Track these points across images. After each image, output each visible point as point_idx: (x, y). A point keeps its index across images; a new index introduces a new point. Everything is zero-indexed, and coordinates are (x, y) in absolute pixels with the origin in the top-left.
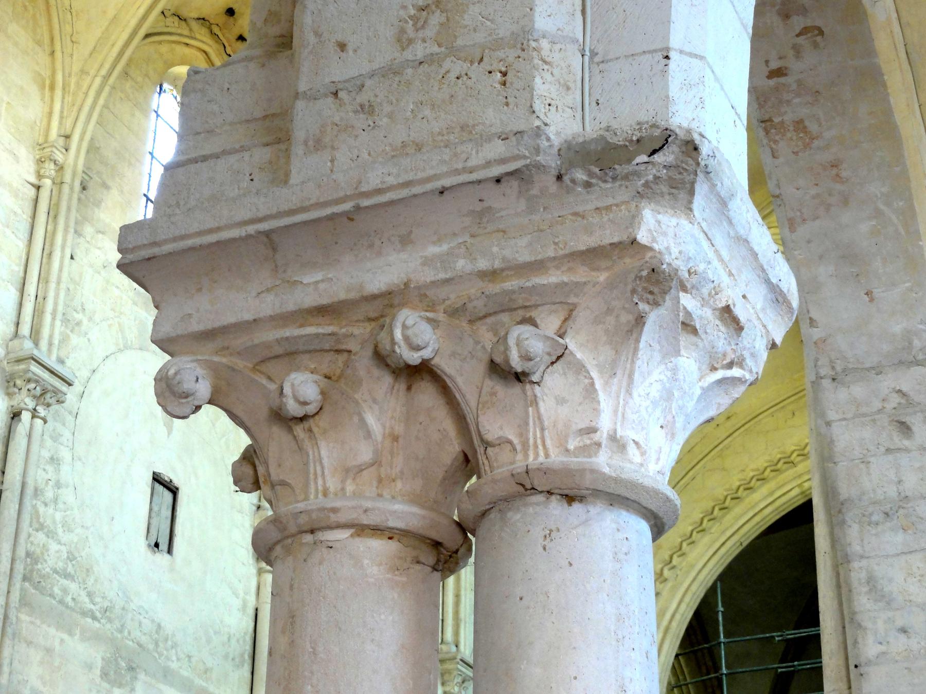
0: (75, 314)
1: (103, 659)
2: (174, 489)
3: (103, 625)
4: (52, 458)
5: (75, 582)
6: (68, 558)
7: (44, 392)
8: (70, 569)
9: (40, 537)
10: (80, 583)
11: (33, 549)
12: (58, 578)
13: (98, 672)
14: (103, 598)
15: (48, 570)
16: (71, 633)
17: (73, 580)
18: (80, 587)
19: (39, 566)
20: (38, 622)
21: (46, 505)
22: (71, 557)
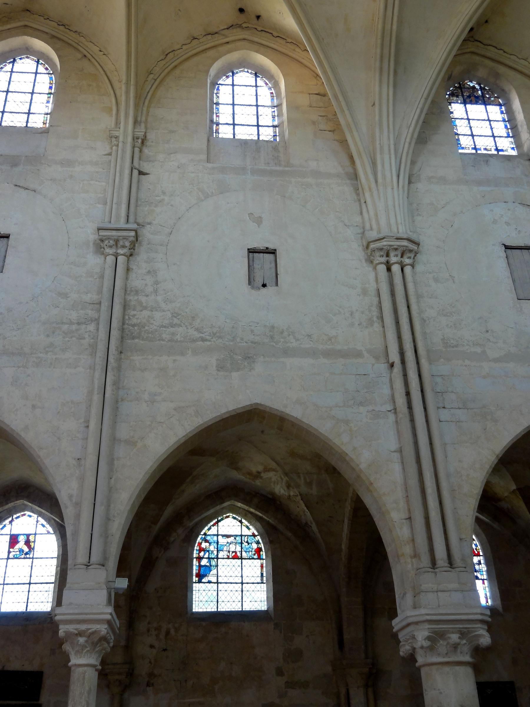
0: (157, 198)
1: (217, 360)
2: (273, 251)
3: (214, 342)
4: (149, 272)
5: (182, 327)
6: (173, 316)
7: (117, 241)
8: (176, 321)
9: (146, 313)
10: (186, 326)
11: (139, 321)
12: (165, 329)
13: (215, 368)
14: (211, 328)
15: (155, 327)
16: (182, 354)
17: (180, 326)
18: (187, 328)
19: (147, 328)
20: (150, 357)
21: (147, 296)
22: (175, 315)
